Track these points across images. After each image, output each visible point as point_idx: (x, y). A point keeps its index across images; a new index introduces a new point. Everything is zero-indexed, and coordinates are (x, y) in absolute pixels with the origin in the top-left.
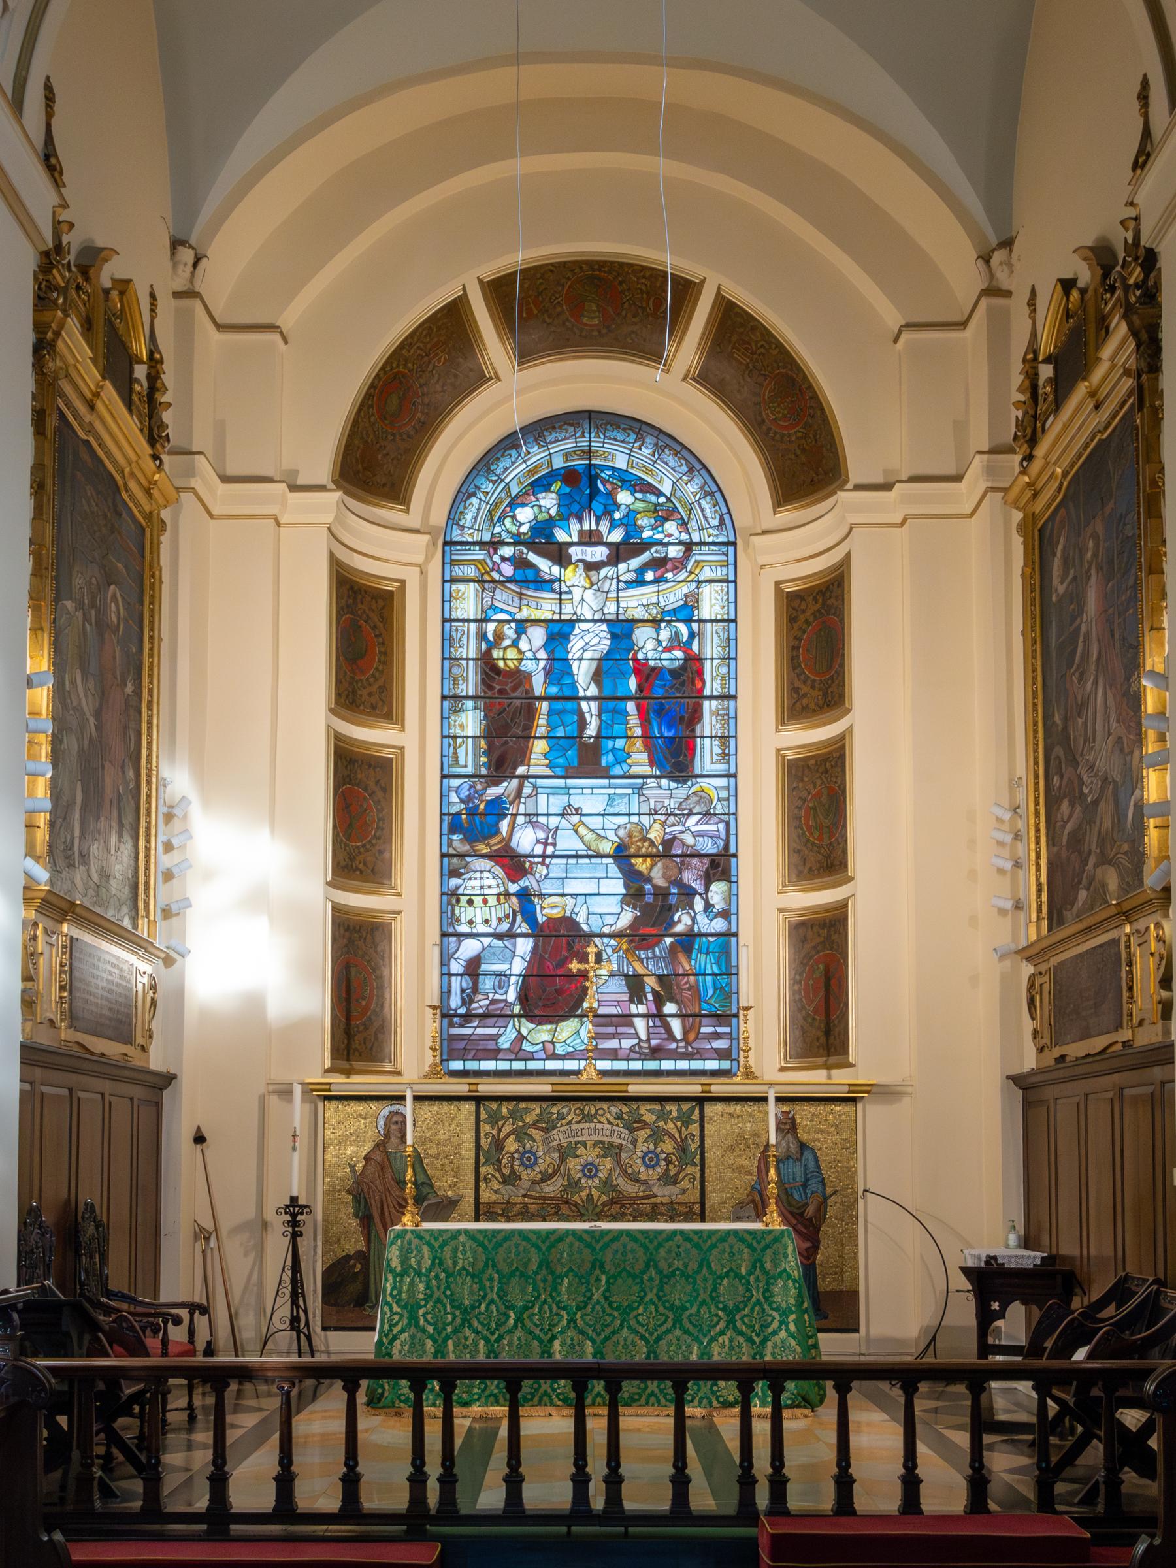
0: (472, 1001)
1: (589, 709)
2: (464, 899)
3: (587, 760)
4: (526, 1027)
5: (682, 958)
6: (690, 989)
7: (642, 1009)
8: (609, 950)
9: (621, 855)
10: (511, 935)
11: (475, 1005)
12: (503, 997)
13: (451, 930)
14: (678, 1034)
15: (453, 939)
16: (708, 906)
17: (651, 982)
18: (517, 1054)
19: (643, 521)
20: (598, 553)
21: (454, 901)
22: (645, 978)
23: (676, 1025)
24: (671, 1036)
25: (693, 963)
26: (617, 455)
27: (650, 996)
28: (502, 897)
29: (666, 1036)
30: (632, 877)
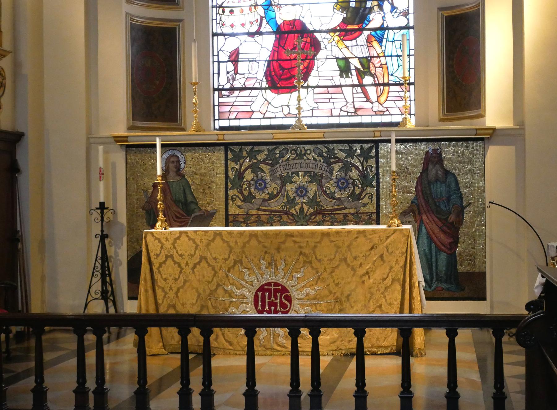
0: (234, 80)
2: (227, 10)
5: (375, 44)
6: (381, 66)
7: (349, 81)
8: (326, 41)
10: (259, 33)
11: (235, 82)
12: (255, 76)
13: (219, 31)
14: (373, 98)
15: (221, 38)
16: (393, 8)
17: (355, 63)
18: (264, 114)
21: (221, 12)
22: (350, 60)
23: (372, 91)
24: (368, 100)
25: (383, 48)
27: (354, 72)
28: (253, 8)
29: (365, 99)
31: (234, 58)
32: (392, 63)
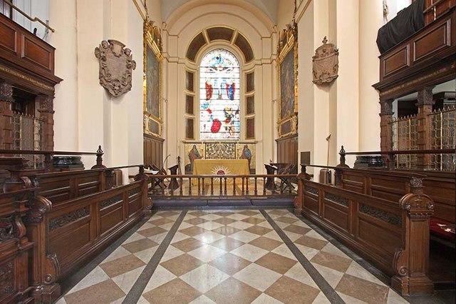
3: (220, 98)
9: (224, 110)
20: (222, 69)
26: (224, 55)
30: (226, 113)
32: (235, 128)
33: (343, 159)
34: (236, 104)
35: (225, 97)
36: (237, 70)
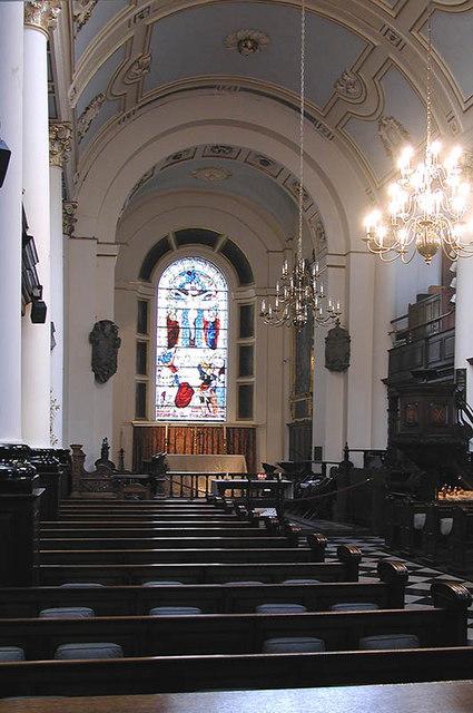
1: (193, 331)
3: (192, 345)
4: (176, 408)
19: (207, 285)
20: (196, 293)
26: (200, 267)
30: (202, 373)
31: (164, 394)
33: (346, 456)
34: (220, 357)
35: (202, 342)
36: (223, 296)
